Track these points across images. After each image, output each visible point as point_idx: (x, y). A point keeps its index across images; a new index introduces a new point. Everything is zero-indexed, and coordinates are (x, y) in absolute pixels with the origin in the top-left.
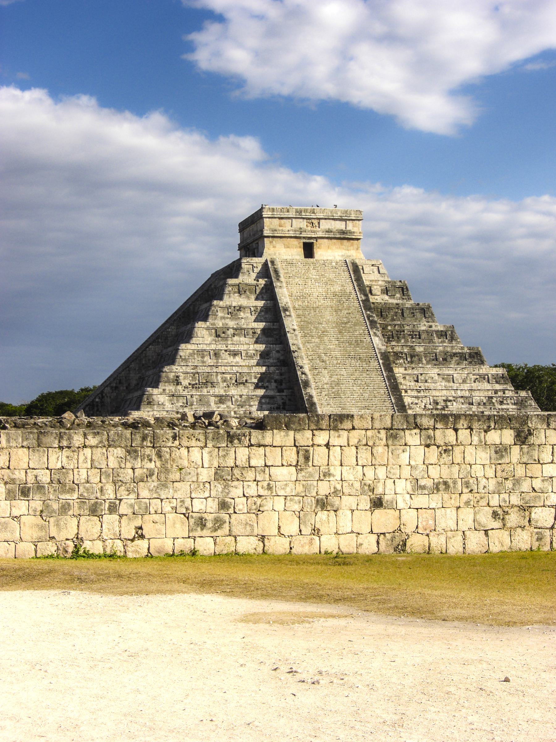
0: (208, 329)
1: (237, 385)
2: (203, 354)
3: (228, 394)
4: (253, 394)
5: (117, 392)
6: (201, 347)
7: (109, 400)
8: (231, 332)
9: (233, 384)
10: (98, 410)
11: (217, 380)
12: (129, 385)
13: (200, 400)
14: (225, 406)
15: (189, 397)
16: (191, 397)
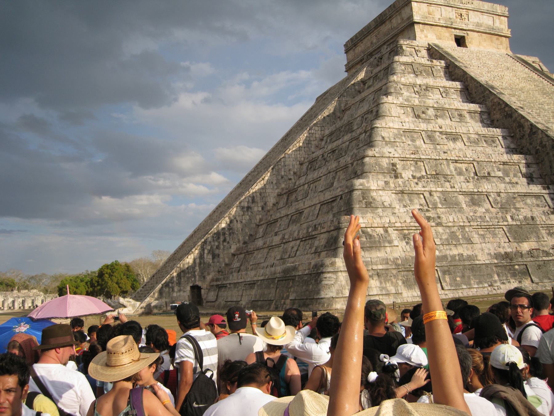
0: (402, 106)
1: (478, 179)
2: (412, 137)
3: (480, 190)
4: (513, 191)
5: (250, 213)
6: (406, 126)
7: (239, 226)
8: (431, 112)
9: (473, 178)
10: (225, 240)
11: (451, 172)
12: (265, 204)
13: (445, 200)
14: (484, 211)
15: (427, 195)
16: (431, 195)
